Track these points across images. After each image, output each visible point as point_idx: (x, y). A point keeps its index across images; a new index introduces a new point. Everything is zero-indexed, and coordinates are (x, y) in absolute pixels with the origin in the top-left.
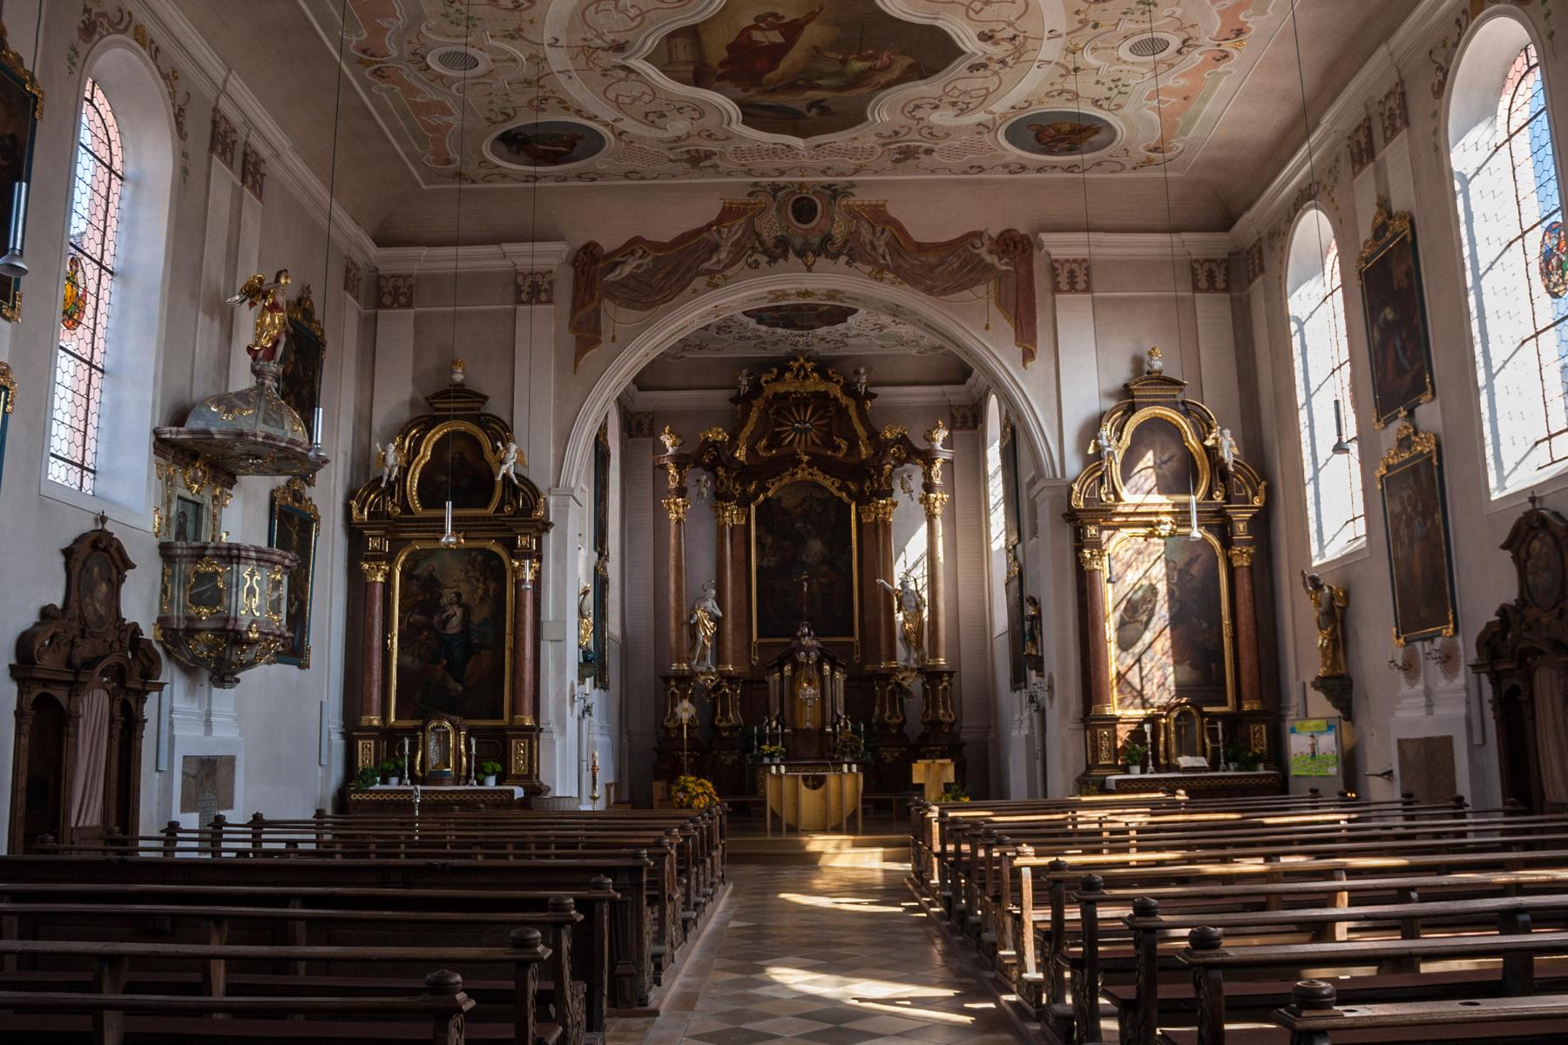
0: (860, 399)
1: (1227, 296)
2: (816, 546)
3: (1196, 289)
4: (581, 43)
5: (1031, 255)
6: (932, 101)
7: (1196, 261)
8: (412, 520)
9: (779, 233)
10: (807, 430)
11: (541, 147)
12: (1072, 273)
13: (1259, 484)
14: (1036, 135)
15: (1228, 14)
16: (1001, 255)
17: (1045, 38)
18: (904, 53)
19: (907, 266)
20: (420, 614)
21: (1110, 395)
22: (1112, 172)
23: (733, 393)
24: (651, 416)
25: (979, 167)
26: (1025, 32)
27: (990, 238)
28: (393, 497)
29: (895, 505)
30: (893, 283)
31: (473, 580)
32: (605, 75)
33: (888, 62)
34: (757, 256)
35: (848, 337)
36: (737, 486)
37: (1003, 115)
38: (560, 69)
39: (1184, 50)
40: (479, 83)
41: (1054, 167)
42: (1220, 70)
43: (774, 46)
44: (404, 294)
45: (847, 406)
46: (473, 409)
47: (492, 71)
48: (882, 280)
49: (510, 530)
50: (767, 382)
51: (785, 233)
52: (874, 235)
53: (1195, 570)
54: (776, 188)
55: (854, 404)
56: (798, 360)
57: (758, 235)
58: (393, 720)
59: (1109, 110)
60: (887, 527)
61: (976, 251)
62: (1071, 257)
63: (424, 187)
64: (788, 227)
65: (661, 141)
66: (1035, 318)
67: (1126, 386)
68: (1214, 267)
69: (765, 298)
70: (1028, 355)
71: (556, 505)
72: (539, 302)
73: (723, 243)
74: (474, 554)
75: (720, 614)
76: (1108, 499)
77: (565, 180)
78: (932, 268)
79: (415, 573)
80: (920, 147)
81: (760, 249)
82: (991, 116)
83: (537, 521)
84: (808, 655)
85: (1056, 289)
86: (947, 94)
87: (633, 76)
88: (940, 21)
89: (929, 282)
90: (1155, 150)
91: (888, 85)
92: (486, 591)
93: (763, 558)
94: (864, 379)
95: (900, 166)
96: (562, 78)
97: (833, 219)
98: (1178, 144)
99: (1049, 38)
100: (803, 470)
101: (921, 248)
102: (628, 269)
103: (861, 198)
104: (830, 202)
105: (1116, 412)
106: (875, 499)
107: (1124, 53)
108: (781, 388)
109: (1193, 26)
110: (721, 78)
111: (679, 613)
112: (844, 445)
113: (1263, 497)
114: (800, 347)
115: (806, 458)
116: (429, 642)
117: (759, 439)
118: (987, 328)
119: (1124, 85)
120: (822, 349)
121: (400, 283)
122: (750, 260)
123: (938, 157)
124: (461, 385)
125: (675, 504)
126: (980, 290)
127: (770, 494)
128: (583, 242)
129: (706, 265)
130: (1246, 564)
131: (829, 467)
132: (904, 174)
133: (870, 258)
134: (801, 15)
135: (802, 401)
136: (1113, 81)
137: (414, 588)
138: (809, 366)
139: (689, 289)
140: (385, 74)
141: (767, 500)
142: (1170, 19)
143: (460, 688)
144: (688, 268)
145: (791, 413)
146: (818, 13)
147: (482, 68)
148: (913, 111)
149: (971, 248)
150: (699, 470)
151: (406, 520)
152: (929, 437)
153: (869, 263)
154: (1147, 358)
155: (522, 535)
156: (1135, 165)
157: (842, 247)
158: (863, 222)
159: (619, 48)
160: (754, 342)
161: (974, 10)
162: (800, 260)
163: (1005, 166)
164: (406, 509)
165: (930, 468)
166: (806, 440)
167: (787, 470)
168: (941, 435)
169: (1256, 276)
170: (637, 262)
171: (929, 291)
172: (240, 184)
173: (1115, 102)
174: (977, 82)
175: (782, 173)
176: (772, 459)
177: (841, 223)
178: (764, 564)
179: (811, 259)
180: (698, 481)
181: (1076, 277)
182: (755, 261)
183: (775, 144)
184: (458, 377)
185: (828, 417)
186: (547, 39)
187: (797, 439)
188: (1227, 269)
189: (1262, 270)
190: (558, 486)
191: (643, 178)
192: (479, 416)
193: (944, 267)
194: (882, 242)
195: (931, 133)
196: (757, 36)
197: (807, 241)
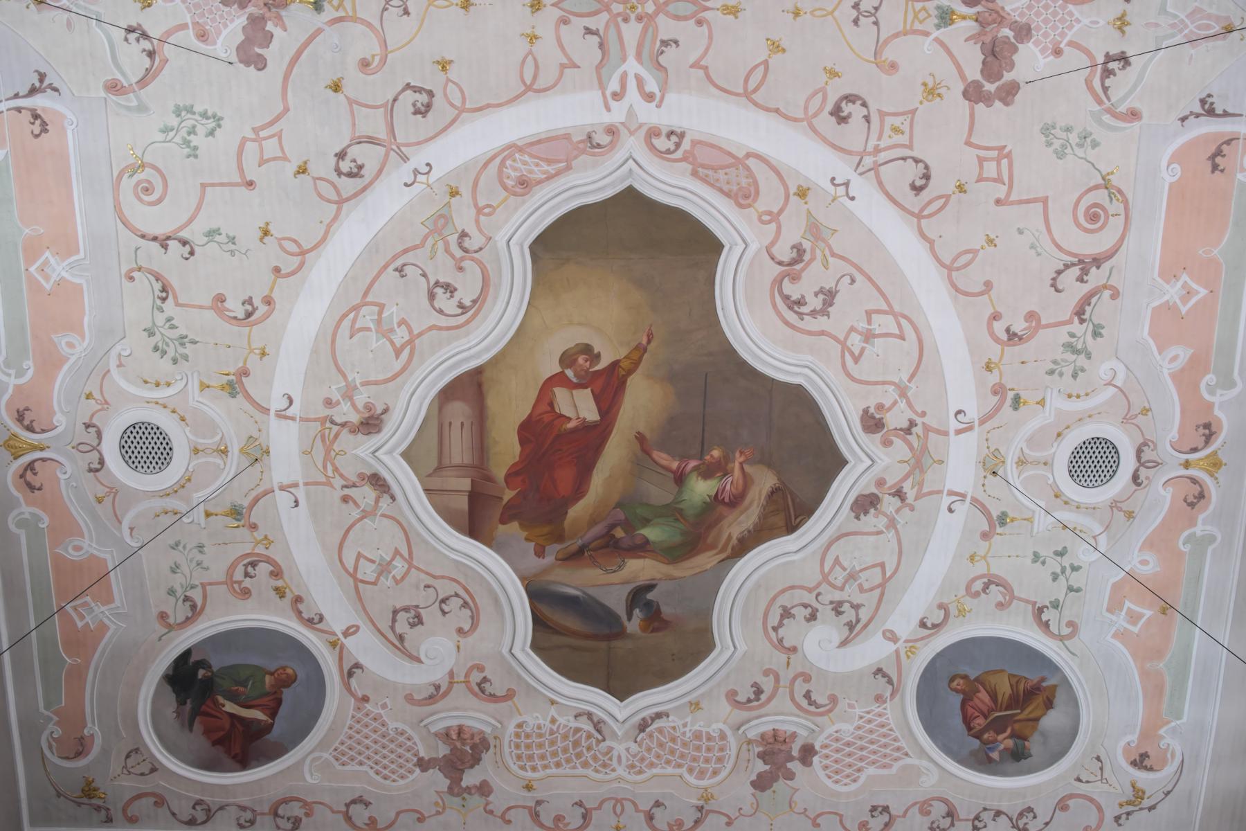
4: (325, 412)
11: (230, 707)
15: (1187, 379)
17: (952, 433)
18: (766, 460)
25: (886, 809)
26: (924, 414)
33: (741, 482)
37: (912, 646)
39: (1143, 473)
42: (1199, 529)
43: (586, 427)
65: (409, 699)
87: (385, 502)
91: (743, 547)
96: (284, 500)
98: (1170, 741)
99: (959, 432)
109: (1145, 411)
123: (821, 774)
134: (621, 353)
146: (645, 350)
148: (781, 625)
161: (852, 354)
186: (277, 403)
195: (807, 695)
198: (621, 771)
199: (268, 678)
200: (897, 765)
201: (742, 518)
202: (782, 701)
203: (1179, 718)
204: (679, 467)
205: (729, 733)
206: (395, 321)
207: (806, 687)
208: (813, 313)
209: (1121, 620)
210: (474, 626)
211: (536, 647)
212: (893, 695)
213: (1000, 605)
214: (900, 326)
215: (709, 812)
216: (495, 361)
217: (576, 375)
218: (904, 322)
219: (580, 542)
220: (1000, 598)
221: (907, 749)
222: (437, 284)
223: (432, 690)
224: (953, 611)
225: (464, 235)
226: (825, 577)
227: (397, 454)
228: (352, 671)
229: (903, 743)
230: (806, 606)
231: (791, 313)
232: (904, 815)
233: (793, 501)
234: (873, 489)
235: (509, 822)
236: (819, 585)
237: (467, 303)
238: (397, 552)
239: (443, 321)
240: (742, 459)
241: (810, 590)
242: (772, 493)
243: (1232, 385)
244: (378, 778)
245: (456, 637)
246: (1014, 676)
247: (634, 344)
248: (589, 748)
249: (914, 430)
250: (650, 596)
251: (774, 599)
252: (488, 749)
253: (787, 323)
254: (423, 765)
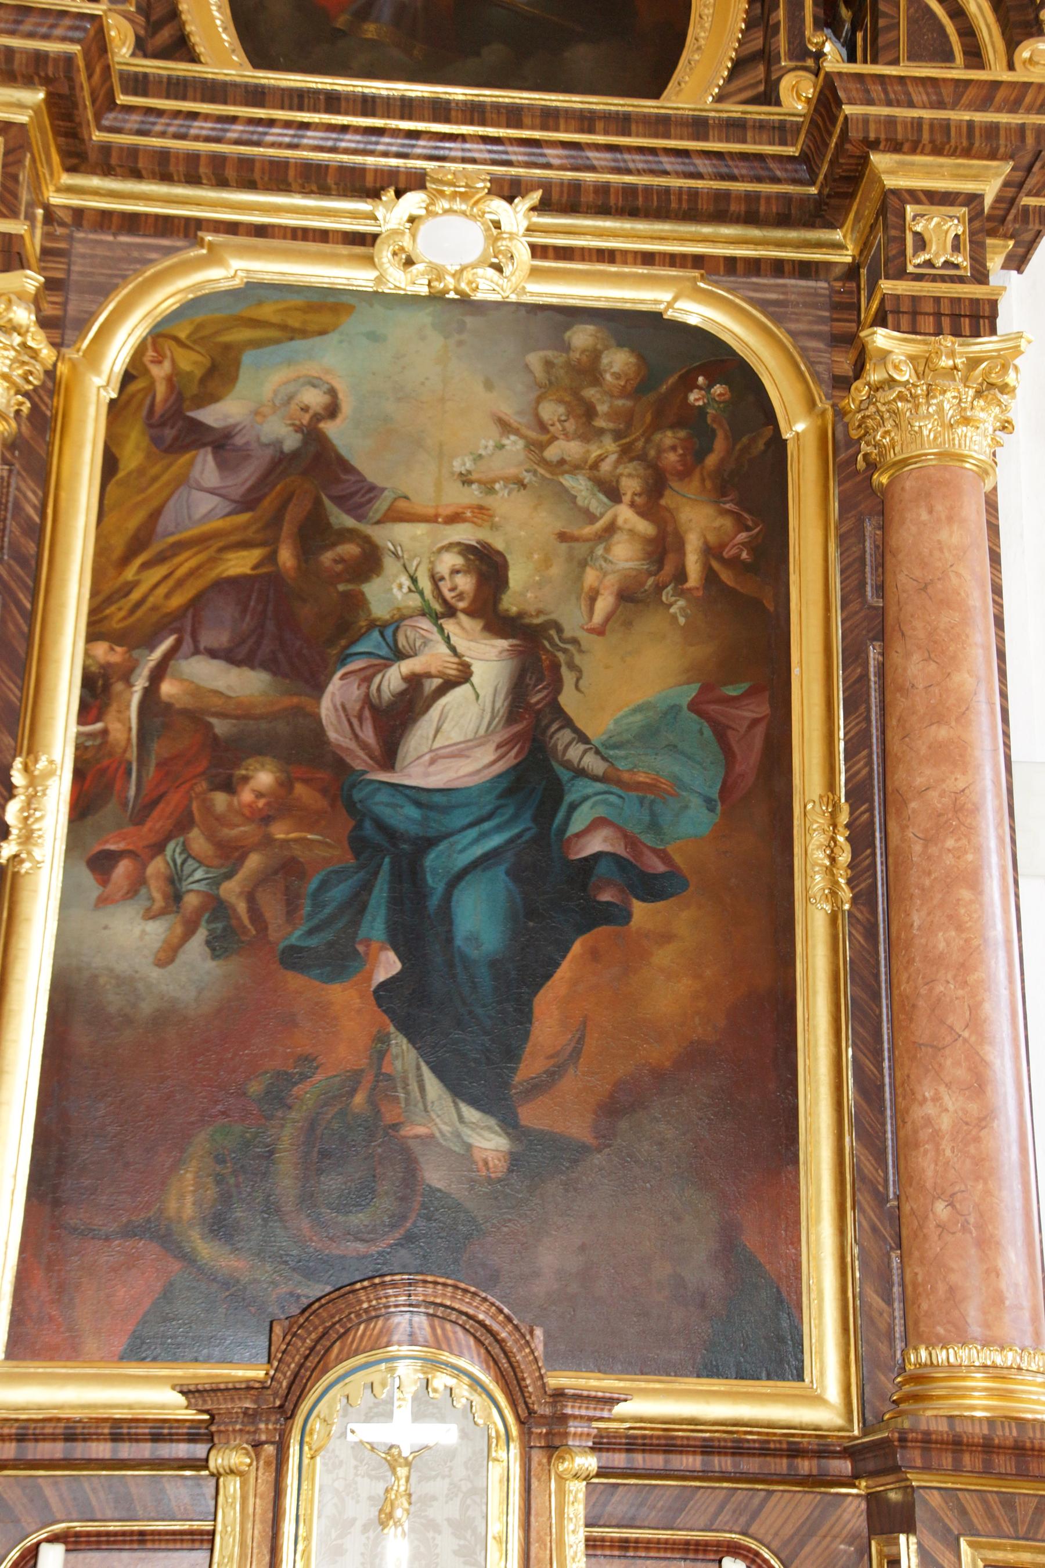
20: (229, 656)
31: (579, 485)
74: (582, 337)
79: (212, 415)
116: (280, 832)
137: (204, 504)
151: (177, 88)
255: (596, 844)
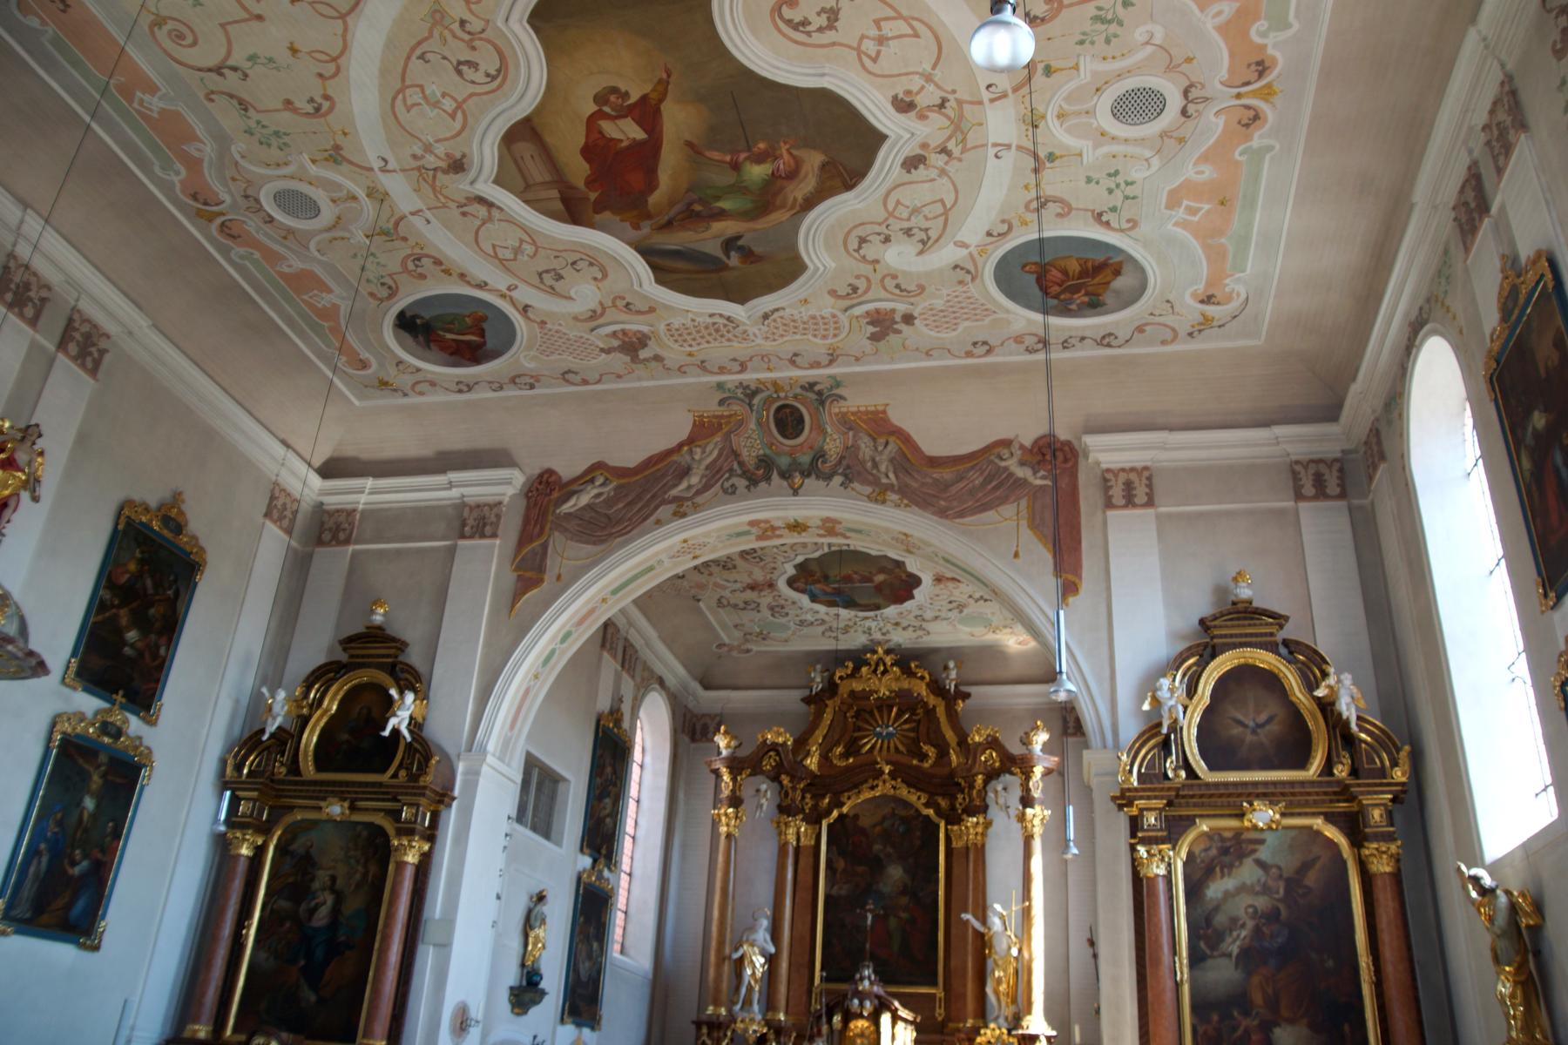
0: (952, 698)
1: (1342, 504)
2: (895, 873)
3: (1299, 496)
4: (415, 164)
5: (1076, 465)
6: (877, 229)
7: (1297, 462)
8: (296, 783)
9: (761, 452)
10: (890, 735)
11: (449, 336)
12: (1129, 486)
13: (1398, 750)
14: (1039, 281)
15: (1235, 30)
16: (1036, 467)
18: (809, 144)
19: (915, 485)
21: (1184, 638)
22: (1164, 343)
23: (806, 693)
24: (718, 719)
26: (954, 92)
27: (1022, 447)
28: (283, 756)
29: (988, 825)
30: (897, 506)
32: (464, 214)
33: (792, 163)
34: (735, 480)
35: (924, 620)
36: (807, 800)
37: (983, 250)
38: (413, 210)
39: (1191, 109)
40: (335, 239)
41: (1083, 339)
43: (636, 145)
44: (344, 530)
45: (934, 707)
46: (388, 656)
47: (339, 218)
48: (884, 502)
49: (395, 799)
50: (841, 678)
51: (768, 452)
52: (876, 449)
53: (1311, 879)
54: (750, 393)
55: (943, 703)
56: (874, 652)
57: (736, 454)
58: (229, 1032)
59: (1122, 231)
60: (981, 851)
61: (1003, 464)
62: (1127, 466)
63: (357, 403)
64: (772, 444)
65: (576, 318)
66: (1080, 542)
67: (1202, 622)
68: (1323, 468)
69: (747, 533)
70: (1069, 589)
71: (466, 773)
72: (483, 536)
73: (695, 466)
75: (772, 950)
76: (1177, 776)
77: (501, 388)
78: (947, 486)
80: (893, 311)
81: (739, 472)
82: (965, 252)
83: (425, 788)
84: (861, 1005)
85: (1109, 504)
86: (891, 214)
87: (495, 213)
88: (827, 78)
89: (942, 503)
90: (1208, 300)
91: (809, 204)
92: (365, 875)
93: (832, 887)
94: (953, 674)
95: (882, 344)
96: (418, 222)
97: (824, 432)
98: (1237, 286)
99: (992, 101)
100: (884, 782)
101: (934, 462)
102: (584, 499)
103: (856, 401)
104: (818, 409)
105: (1188, 658)
106: (964, 816)
107: (1105, 121)
108: (857, 686)
109: (1189, 60)
110: (599, 207)
111: (721, 943)
112: (931, 752)
113: (1407, 767)
114: (878, 636)
115: (887, 769)
117: (835, 745)
118: (1016, 555)
119: (1127, 184)
120: (900, 638)
121: (342, 518)
122: (727, 485)
123: (925, 330)
124: (380, 628)
125: (726, 815)
126: (1008, 510)
127: (845, 810)
128: (537, 471)
129: (674, 492)
130: (1388, 869)
131: (914, 780)
132: (892, 360)
133: (871, 478)
134: (647, 88)
135: (884, 705)
136: (1109, 175)
138: (888, 660)
139: (652, 519)
140: (234, 232)
141: (841, 817)
142: (1149, 49)
143: (313, 998)
144: (653, 497)
145: (871, 713)
146: (668, 83)
147: (328, 213)
148: (860, 247)
149: (997, 461)
150: (760, 778)
152: (1025, 740)
153: (869, 483)
154: (1232, 585)
155: (410, 805)
156: (1191, 330)
157: (836, 465)
158: (861, 434)
159: (457, 166)
160: (821, 629)
161: (869, 56)
162: (785, 483)
163: (1018, 339)
164: (294, 767)
165: (1028, 778)
166: (889, 747)
167: (866, 781)
168: (1041, 738)
169: (1375, 468)
170: (595, 491)
171: (942, 513)
172: (52, 348)
173: (1125, 215)
174: (923, 191)
175: (743, 368)
176: (848, 768)
177: (835, 436)
178: (834, 891)
179: (798, 480)
180: (758, 791)
181: (1135, 488)
182: (733, 485)
183: (711, 315)
184: (378, 618)
185: (915, 721)
187: (878, 745)
188: (1341, 470)
189: (1383, 457)
190: (470, 750)
191: (585, 382)
192: (394, 665)
193: (961, 485)
194: (884, 457)
195: (898, 286)
196: (610, 129)
197: (794, 459)
198: (759, 341)
199: (467, 319)
200: (987, 320)
201: (802, 185)
202: (876, 292)
203: (1243, 271)
204: (732, 160)
205: (839, 314)
206: (439, 94)
207: (895, 282)
208: (820, 30)
209: (1180, 213)
210: (605, 275)
211: (659, 281)
212: (973, 279)
213: (1059, 215)
214: (912, 28)
215: (838, 356)
216: (539, 110)
217: (613, 109)
218: (915, 23)
219: (666, 218)
220: (1060, 210)
221: (993, 309)
222: (460, 63)
223: (590, 313)
224: (1016, 223)
225: (463, 23)
226: (891, 214)
227: (490, 183)
228: (525, 309)
229: (989, 306)
230: (879, 234)
231: (798, 34)
232: (1002, 344)
233: (845, 169)
234: (919, 151)
235: (685, 373)
236: (886, 219)
237: (493, 72)
238: (522, 241)
239: (479, 89)
240: (787, 146)
241: (880, 224)
242: (824, 165)
243: (1288, 26)
244: (577, 361)
245: (593, 282)
246: (1081, 259)
247: (656, 80)
248: (728, 332)
249: (947, 104)
250: (740, 243)
251: (849, 232)
252: (650, 339)
253: (796, 42)
254: (608, 351)
255: (343, 938)
